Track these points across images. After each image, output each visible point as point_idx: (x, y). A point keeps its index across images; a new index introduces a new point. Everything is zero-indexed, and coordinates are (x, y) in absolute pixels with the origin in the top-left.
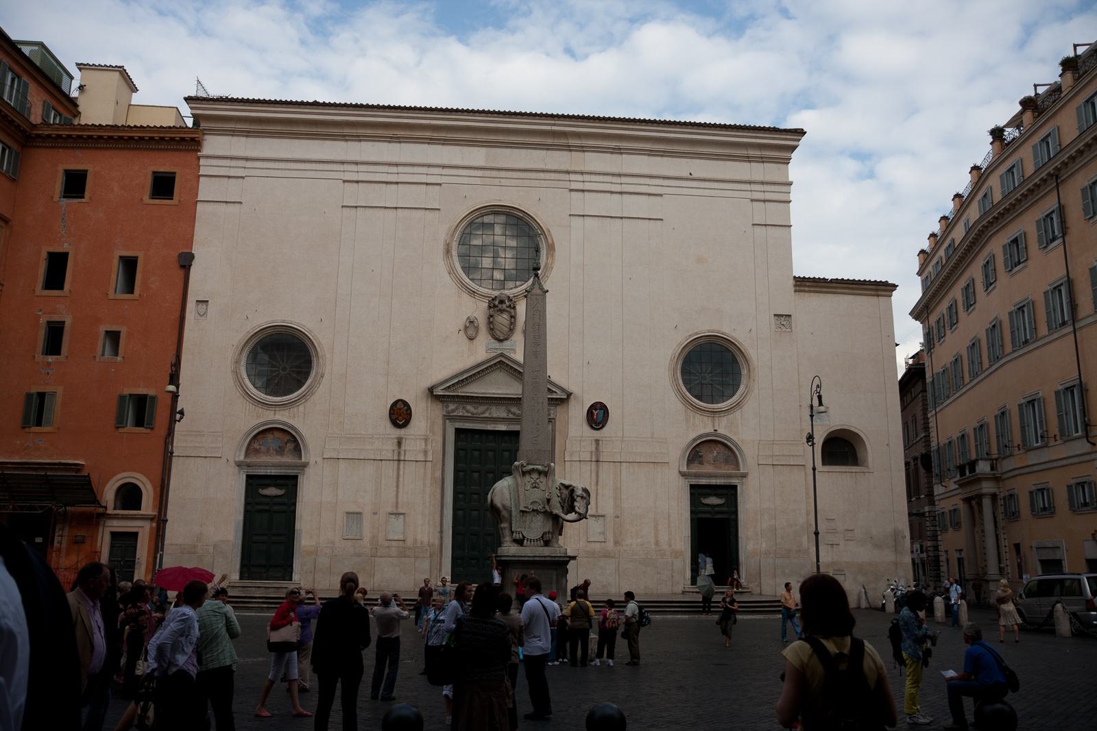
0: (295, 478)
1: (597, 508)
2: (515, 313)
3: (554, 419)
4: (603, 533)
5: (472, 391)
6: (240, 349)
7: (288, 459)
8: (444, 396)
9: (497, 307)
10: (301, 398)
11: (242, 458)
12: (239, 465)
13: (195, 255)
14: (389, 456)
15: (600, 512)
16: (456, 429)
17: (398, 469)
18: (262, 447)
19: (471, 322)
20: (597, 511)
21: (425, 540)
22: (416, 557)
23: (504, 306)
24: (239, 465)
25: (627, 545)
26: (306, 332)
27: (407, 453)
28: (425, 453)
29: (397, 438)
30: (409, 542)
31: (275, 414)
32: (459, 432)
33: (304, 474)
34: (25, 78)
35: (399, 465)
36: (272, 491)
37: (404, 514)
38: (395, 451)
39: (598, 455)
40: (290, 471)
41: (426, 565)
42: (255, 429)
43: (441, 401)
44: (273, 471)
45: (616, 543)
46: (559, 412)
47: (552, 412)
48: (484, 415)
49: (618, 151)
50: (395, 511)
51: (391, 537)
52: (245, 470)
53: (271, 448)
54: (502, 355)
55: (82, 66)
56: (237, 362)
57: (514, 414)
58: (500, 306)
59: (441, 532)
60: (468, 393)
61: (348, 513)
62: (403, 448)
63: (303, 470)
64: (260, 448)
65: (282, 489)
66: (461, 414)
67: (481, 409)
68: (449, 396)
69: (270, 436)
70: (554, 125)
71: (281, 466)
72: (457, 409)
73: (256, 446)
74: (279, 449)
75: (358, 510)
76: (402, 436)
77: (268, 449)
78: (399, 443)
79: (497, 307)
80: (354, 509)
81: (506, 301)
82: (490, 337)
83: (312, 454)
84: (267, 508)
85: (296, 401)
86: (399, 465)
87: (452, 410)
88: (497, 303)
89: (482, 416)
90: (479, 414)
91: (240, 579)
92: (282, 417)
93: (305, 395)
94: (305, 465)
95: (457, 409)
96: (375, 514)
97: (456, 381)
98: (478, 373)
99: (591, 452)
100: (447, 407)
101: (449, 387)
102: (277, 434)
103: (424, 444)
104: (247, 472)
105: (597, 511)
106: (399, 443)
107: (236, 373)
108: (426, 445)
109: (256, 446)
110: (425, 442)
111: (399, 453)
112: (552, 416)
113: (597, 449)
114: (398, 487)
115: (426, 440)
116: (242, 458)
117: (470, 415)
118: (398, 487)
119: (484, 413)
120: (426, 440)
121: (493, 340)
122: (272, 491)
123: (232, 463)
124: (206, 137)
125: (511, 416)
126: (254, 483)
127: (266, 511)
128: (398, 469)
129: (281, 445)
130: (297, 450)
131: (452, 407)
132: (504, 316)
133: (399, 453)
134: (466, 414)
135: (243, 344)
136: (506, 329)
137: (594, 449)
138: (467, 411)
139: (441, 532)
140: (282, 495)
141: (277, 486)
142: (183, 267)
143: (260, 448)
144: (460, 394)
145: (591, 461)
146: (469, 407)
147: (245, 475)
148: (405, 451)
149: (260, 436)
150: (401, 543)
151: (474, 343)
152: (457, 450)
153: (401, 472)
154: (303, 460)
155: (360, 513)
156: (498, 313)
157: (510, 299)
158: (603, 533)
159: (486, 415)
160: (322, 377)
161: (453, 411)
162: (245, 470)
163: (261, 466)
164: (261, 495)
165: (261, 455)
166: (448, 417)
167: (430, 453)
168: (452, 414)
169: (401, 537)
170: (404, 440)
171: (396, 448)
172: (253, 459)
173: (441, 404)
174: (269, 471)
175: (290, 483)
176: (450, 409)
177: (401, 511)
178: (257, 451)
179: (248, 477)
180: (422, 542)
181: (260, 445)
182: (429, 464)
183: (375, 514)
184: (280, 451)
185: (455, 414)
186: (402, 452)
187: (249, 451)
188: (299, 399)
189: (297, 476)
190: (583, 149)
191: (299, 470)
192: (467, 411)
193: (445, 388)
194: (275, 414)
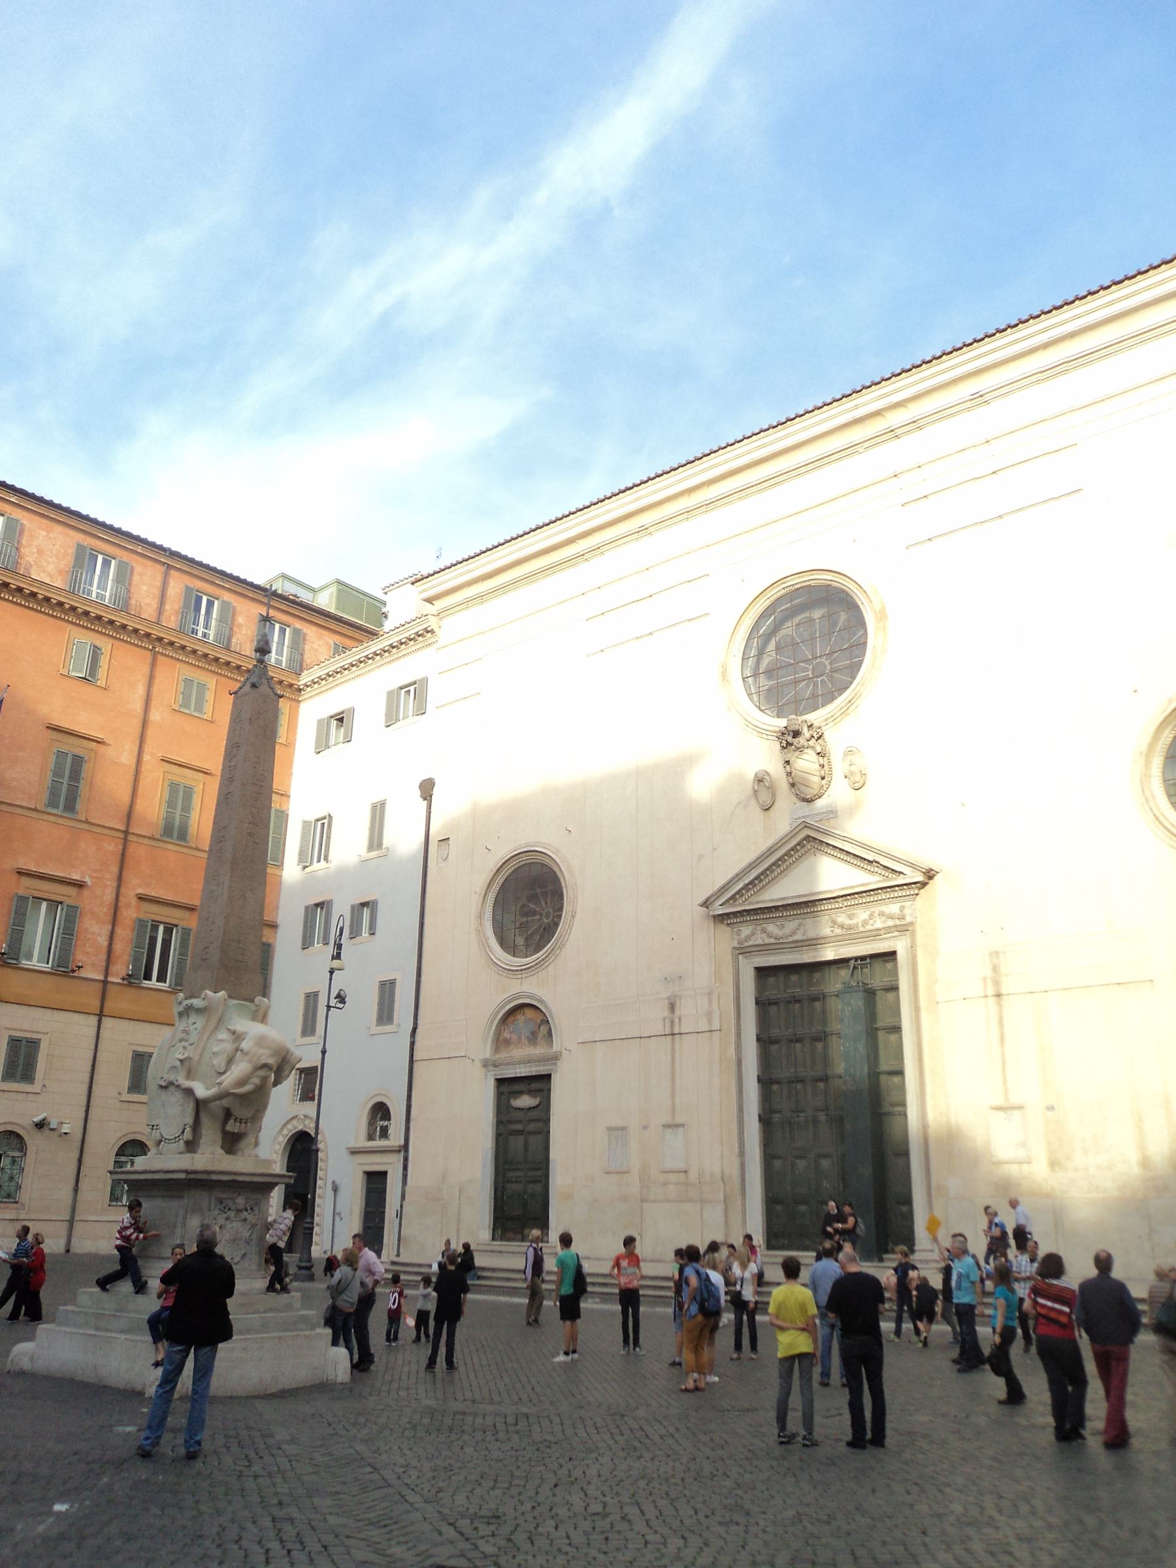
0: (547, 1077)
1: (1006, 1092)
2: (824, 747)
3: (912, 924)
4: (1024, 1145)
5: (770, 898)
6: (483, 893)
7: (539, 1051)
8: (728, 914)
9: (791, 744)
10: (549, 954)
11: (487, 1053)
12: (486, 1064)
13: (436, 781)
14: (659, 1028)
15: (1014, 1100)
16: (755, 968)
17: (673, 1049)
18: (514, 1036)
19: (760, 781)
20: (1007, 1099)
21: (717, 1169)
22: (703, 1201)
23: (801, 740)
24: (486, 1064)
25: (1076, 1170)
26: (552, 855)
27: (683, 1021)
28: (709, 1015)
29: (668, 998)
30: (693, 1176)
31: (521, 983)
32: (762, 973)
33: (556, 1072)
34: (298, 625)
35: (673, 1042)
36: (525, 1101)
37: (683, 1125)
38: (666, 1021)
39: (997, 983)
40: (542, 1068)
41: (715, 1214)
42: (502, 1008)
43: (728, 925)
44: (523, 1070)
45: (1054, 1164)
46: (918, 908)
47: (907, 911)
48: (795, 938)
49: (979, 399)
50: (671, 1122)
51: (670, 1164)
52: (493, 1073)
53: (523, 1036)
54: (807, 826)
55: (387, 590)
56: (480, 916)
57: (842, 927)
58: (795, 741)
59: (742, 1154)
60: (758, 902)
61: (610, 1129)
62: (677, 1013)
63: (556, 1064)
64: (511, 1038)
65: (536, 1098)
66: (759, 942)
67: (791, 926)
68: (735, 914)
69: (521, 1018)
70: (857, 407)
71: (529, 1061)
72: (753, 934)
73: (506, 1034)
74: (531, 1037)
75: (621, 1123)
76: (677, 993)
77: (520, 1039)
78: (672, 1007)
79: (791, 744)
80: (617, 1121)
81: (805, 730)
82: (794, 799)
83: (565, 1037)
84: (519, 1127)
85: (543, 960)
86: (673, 1042)
87: (746, 937)
88: (790, 739)
89: (790, 939)
90: (786, 937)
91: (493, 1239)
92: (530, 988)
93: (553, 949)
94: (556, 1058)
95: (753, 934)
96: (645, 1127)
97: (740, 885)
98: (775, 864)
99: (985, 979)
100: (739, 933)
101: (733, 897)
102: (529, 1013)
103: (707, 1001)
104: (495, 1075)
105: (1007, 1099)
106: (672, 1007)
107: (480, 931)
108: (710, 1004)
109: (506, 1035)
110: (709, 1001)
111: (672, 1022)
112: (908, 919)
113: (995, 969)
114: (673, 1080)
115: (710, 994)
116: (488, 1055)
117: (772, 940)
118: (673, 1080)
119: (794, 933)
120: (710, 994)
121: (800, 804)
122: (525, 1101)
123: (478, 1064)
124: (442, 623)
125: (838, 931)
126: (507, 1087)
127: (521, 1132)
128: (673, 1049)
129: (534, 1029)
130: (550, 1033)
131: (746, 930)
132: (805, 756)
133: (672, 1022)
134: (767, 941)
135: (486, 886)
136: (816, 779)
137: (989, 973)
138: (770, 936)
139: (742, 1154)
140: (537, 1106)
141: (531, 1093)
142: (425, 799)
143: (511, 1038)
144: (747, 908)
145: (987, 996)
146: (771, 928)
147: (491, 1084)
148: (680, 1020)
149: (511, 1019)
150: (682, 1175)
151: (772, 815)
152: (762, 1004)
153: (677, 1056)
154: (556, 1047)
155: (624, 1129)
156: (797, 753)
157: (810, 727)
158: (1024, 1145)
159: (799, 937)
160: (573, 917)
161: (748, 938)
162: (493, 1073)
163: (508, 1064)
164: (516, 1108)
165: (512, 1047)
166: (742, 951)
167: (716, 1016)
168: (746, 944)
169: (681, 1165)
170: (678, 1000)
171: (666, 1013)
172: (503, 1055)
173: (729, 929)
174: (518, 1070)
175: (540, 1083)
176: (743, 936)
177: (679, 1120)
178: (507, 1042)
179: (500, 1082)
180: (712, 1175)
181: (510, 1033)
182: (716, 1035)
183: (645, 1127)
184: (533, 1039)
185: (751, 943)
186: (677, 1020)
187: (500, 1042)
188: (547, 956)
189: (550, 1075)
190: (916, 424)
191: (551, 1064)
192: (770, 936)
193: (727, 901)
194: (521, 983)
